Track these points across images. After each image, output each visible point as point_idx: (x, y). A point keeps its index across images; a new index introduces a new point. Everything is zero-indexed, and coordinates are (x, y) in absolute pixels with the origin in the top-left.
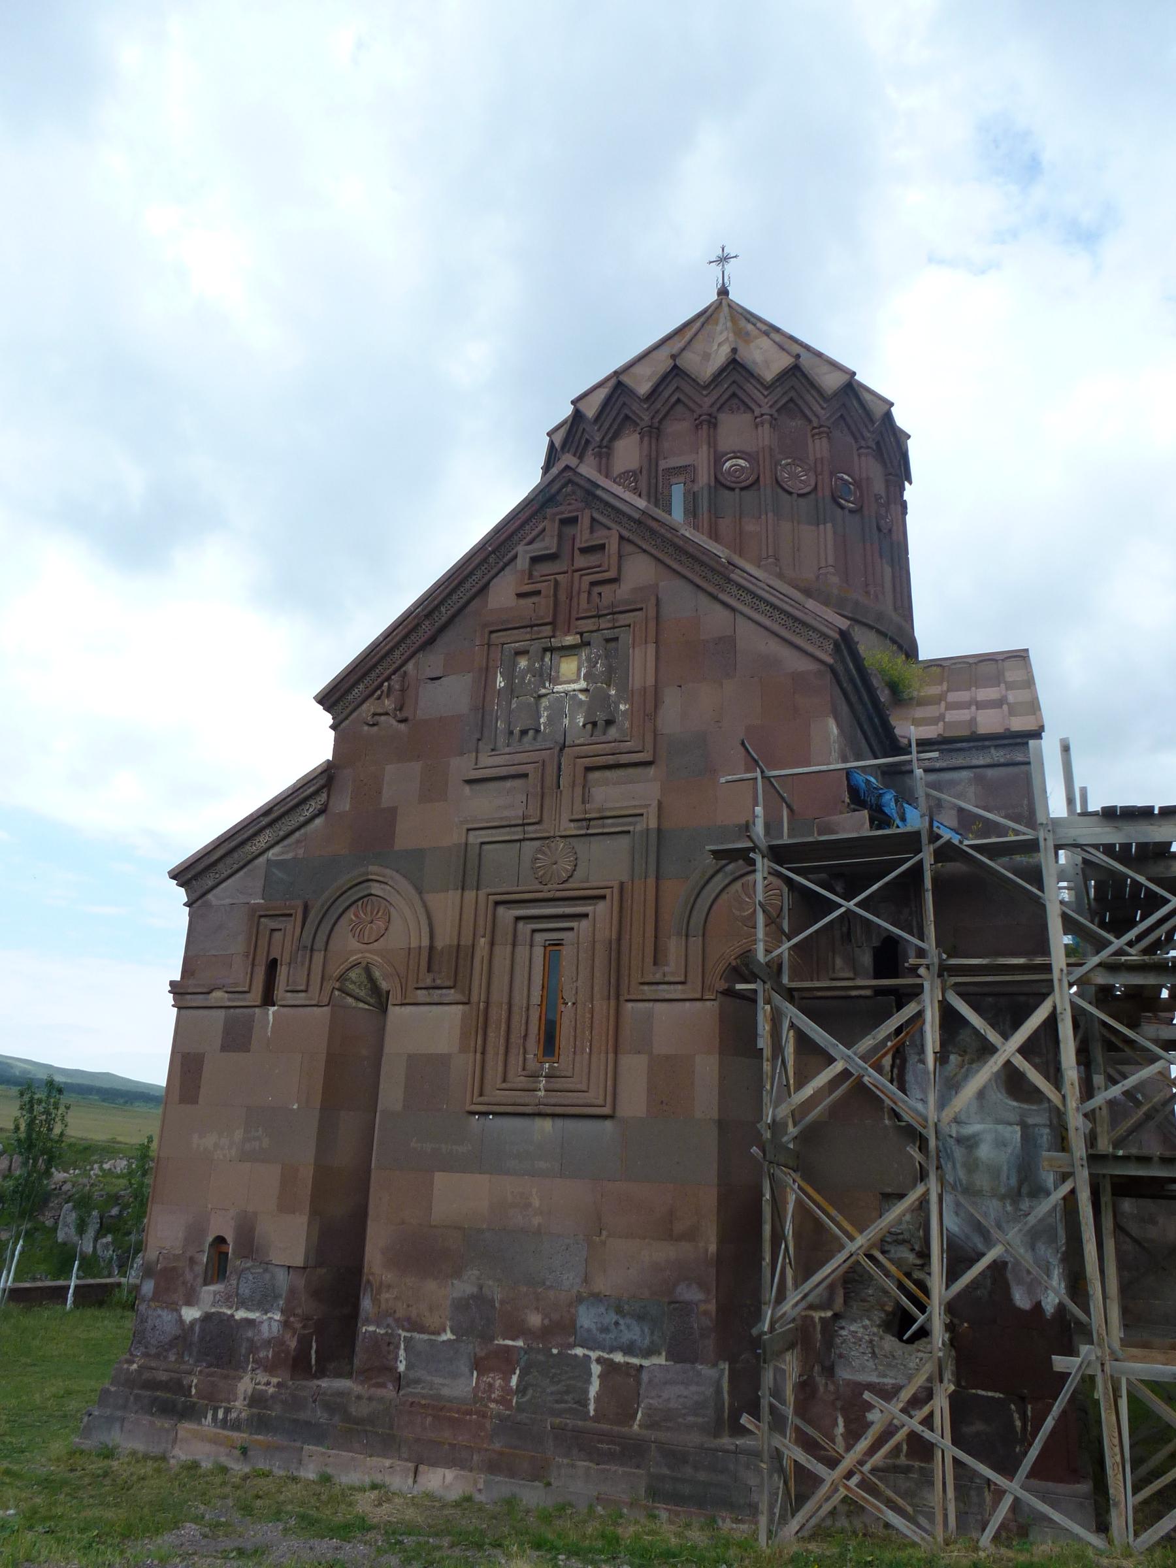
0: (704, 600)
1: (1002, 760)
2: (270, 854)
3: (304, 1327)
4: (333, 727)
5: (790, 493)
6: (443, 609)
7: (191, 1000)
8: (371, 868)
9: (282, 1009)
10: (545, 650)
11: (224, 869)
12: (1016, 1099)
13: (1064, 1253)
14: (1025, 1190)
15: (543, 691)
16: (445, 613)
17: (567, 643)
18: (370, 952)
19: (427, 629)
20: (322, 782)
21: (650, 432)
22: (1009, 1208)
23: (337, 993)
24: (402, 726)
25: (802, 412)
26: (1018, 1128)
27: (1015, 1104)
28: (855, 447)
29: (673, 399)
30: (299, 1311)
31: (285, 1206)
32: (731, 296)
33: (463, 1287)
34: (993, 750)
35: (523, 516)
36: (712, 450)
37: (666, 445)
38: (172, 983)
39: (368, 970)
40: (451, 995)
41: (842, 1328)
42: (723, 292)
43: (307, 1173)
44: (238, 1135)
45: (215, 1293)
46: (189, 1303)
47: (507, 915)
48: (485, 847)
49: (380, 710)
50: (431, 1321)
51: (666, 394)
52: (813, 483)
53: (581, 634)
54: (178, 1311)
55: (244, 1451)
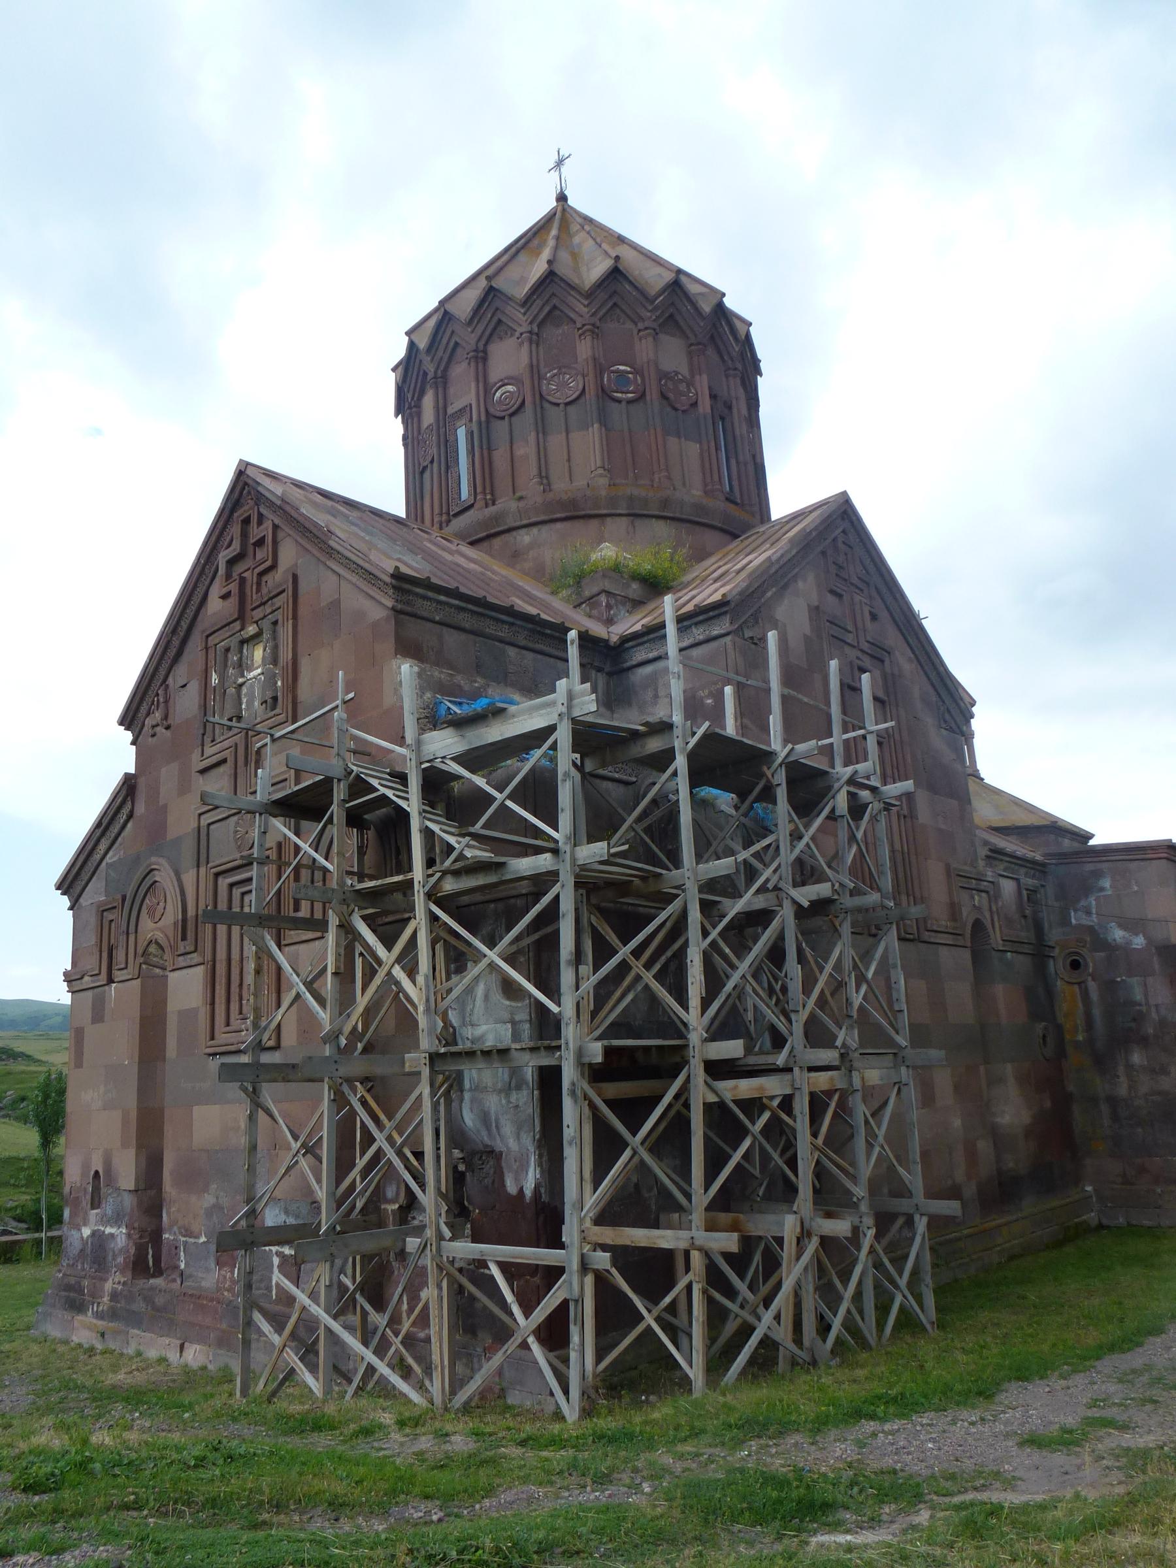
0: (321, 567)
1: (701, 637)
2: (108, 859)
3: (141, 1237)
4: (133, 743)
5: (558, 405)
6: (183, 623)
7: (78, 985)
8: (153, 859)
9: (120, 985)
10: (243, 642)
11: (85, 877)
12: (509, 998)
13: (539, 1141)
14: (513, 1085)
15: (241, 680)
16: (184, 625)
17: (251, 633)
18: (157, 929)
19: (176, 642)
20: (124, 792)
21: (436, 383)
22: (504, 1101)
23: (144, 966)
24: (168, 733)
25: (568, 317)
26: (509, 1026)
27: (508, 1003)
28: (635, 332)
29: (452, 344)
30: (136, 1225)
31: (125, 1145)
32: (570, 202)
33: (209, 1200)
34: (694, 630)
35: (220, 525)
36: (481, 385)
37: (452, 391)
38: (66, 974)
39: (157, 943)
40: (195, 958)
41: (414, 1218)
42: (562, 198)
43: (134, 1115)
44: (102, 1089)
45: (97, 1214)
46: (85, 1225)
47: (224, 882)
48: (212, 827)
49: (154, 723)
50: (195, 1228)
51: (444, 341)
52: (581, 387)
53: (256, 622)
54: (80, 1230)
55: (103, 1335)
